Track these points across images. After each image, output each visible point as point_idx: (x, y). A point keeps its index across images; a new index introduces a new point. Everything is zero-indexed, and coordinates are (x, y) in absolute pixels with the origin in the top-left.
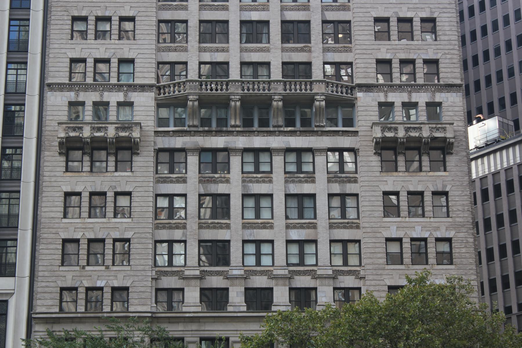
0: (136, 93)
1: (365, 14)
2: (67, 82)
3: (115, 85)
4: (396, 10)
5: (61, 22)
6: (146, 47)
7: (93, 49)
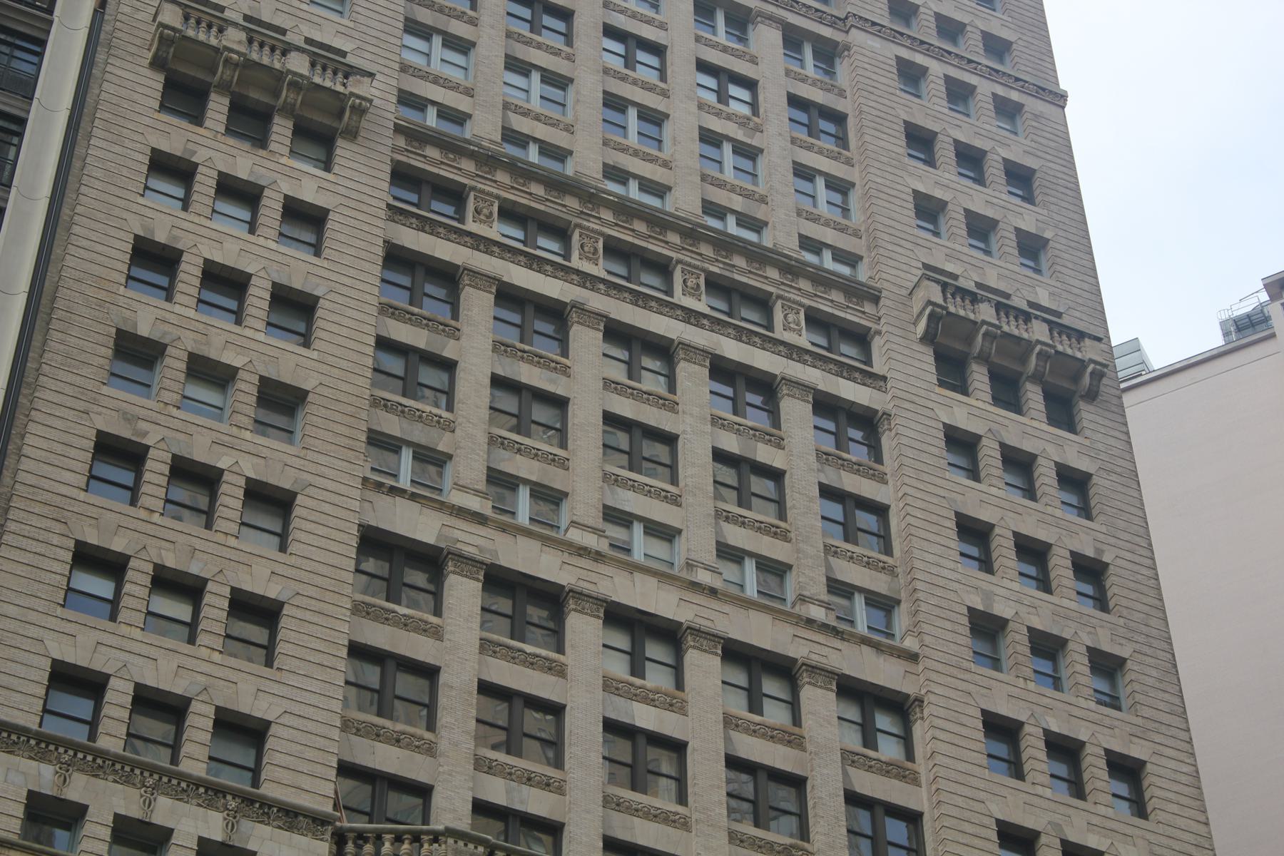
0: (268, 829)
1: (971, 802)
2: (35, 727)
3: (197, 783)
4: (1057, 818)
5: (40, 548)
6: (314, 699)
7: (134, 654)
